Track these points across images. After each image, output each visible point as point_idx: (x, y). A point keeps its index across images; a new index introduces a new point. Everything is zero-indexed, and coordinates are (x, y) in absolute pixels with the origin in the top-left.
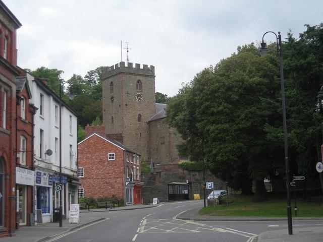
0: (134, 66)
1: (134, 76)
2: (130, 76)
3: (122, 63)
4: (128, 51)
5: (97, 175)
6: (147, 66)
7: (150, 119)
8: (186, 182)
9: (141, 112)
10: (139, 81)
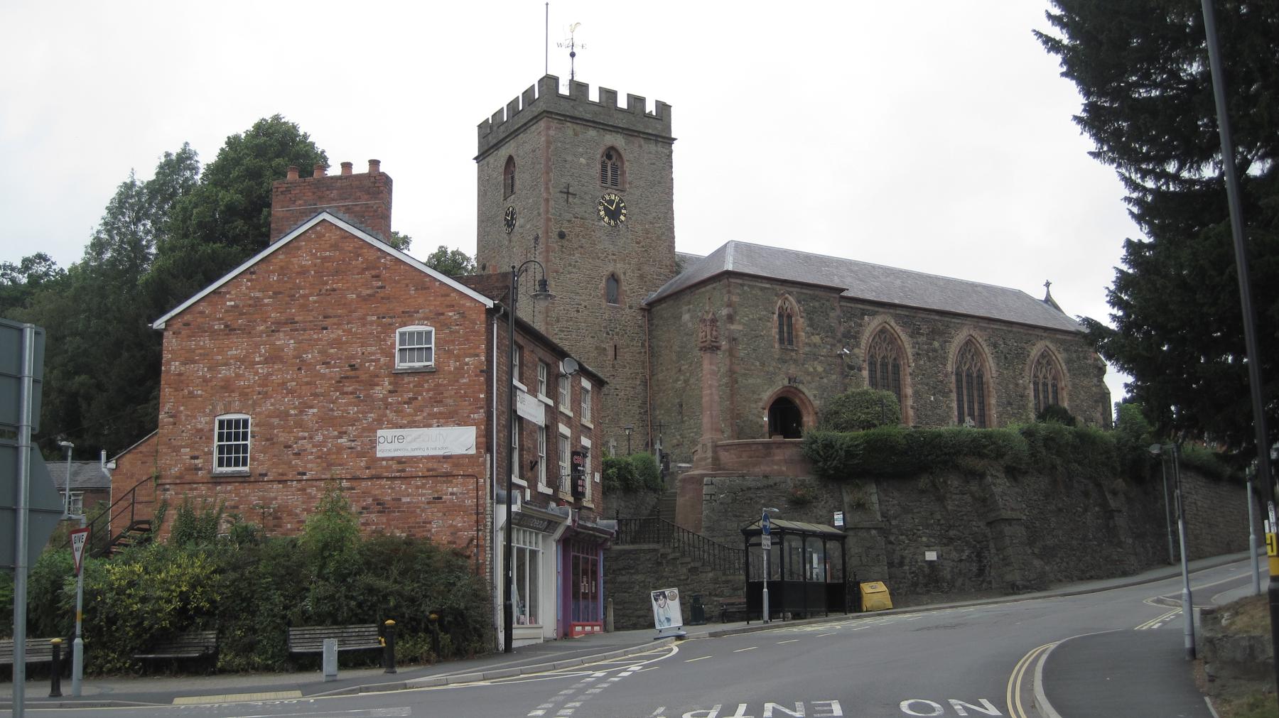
0: (594, 96)
1: (592, 133)
2: (578, 128)
3: (549, 82)
4: (573, 55)
5: (327, 461)
6: (641, 100)
7: (654, 295)
8: (830, 522)
9: (619, 268)
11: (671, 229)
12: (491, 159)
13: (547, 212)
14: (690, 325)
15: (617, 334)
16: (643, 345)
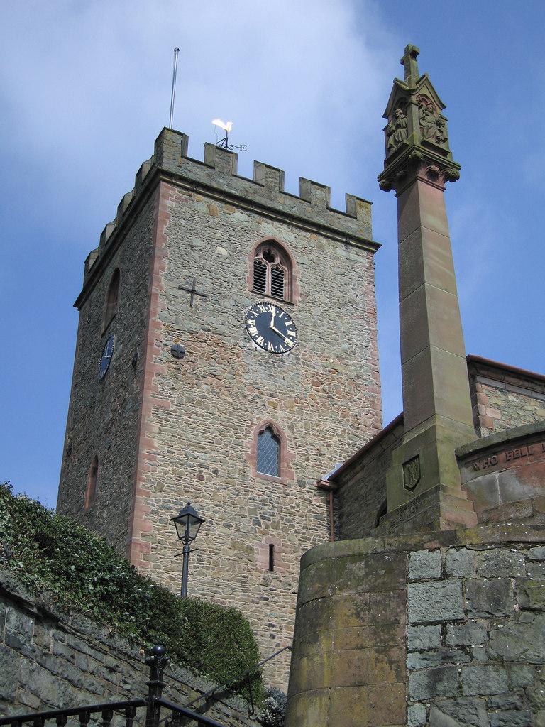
1: (239, 216)
2: (217, 205)
9: (281, 419)
10: (271, 249)
12: (95, 294)
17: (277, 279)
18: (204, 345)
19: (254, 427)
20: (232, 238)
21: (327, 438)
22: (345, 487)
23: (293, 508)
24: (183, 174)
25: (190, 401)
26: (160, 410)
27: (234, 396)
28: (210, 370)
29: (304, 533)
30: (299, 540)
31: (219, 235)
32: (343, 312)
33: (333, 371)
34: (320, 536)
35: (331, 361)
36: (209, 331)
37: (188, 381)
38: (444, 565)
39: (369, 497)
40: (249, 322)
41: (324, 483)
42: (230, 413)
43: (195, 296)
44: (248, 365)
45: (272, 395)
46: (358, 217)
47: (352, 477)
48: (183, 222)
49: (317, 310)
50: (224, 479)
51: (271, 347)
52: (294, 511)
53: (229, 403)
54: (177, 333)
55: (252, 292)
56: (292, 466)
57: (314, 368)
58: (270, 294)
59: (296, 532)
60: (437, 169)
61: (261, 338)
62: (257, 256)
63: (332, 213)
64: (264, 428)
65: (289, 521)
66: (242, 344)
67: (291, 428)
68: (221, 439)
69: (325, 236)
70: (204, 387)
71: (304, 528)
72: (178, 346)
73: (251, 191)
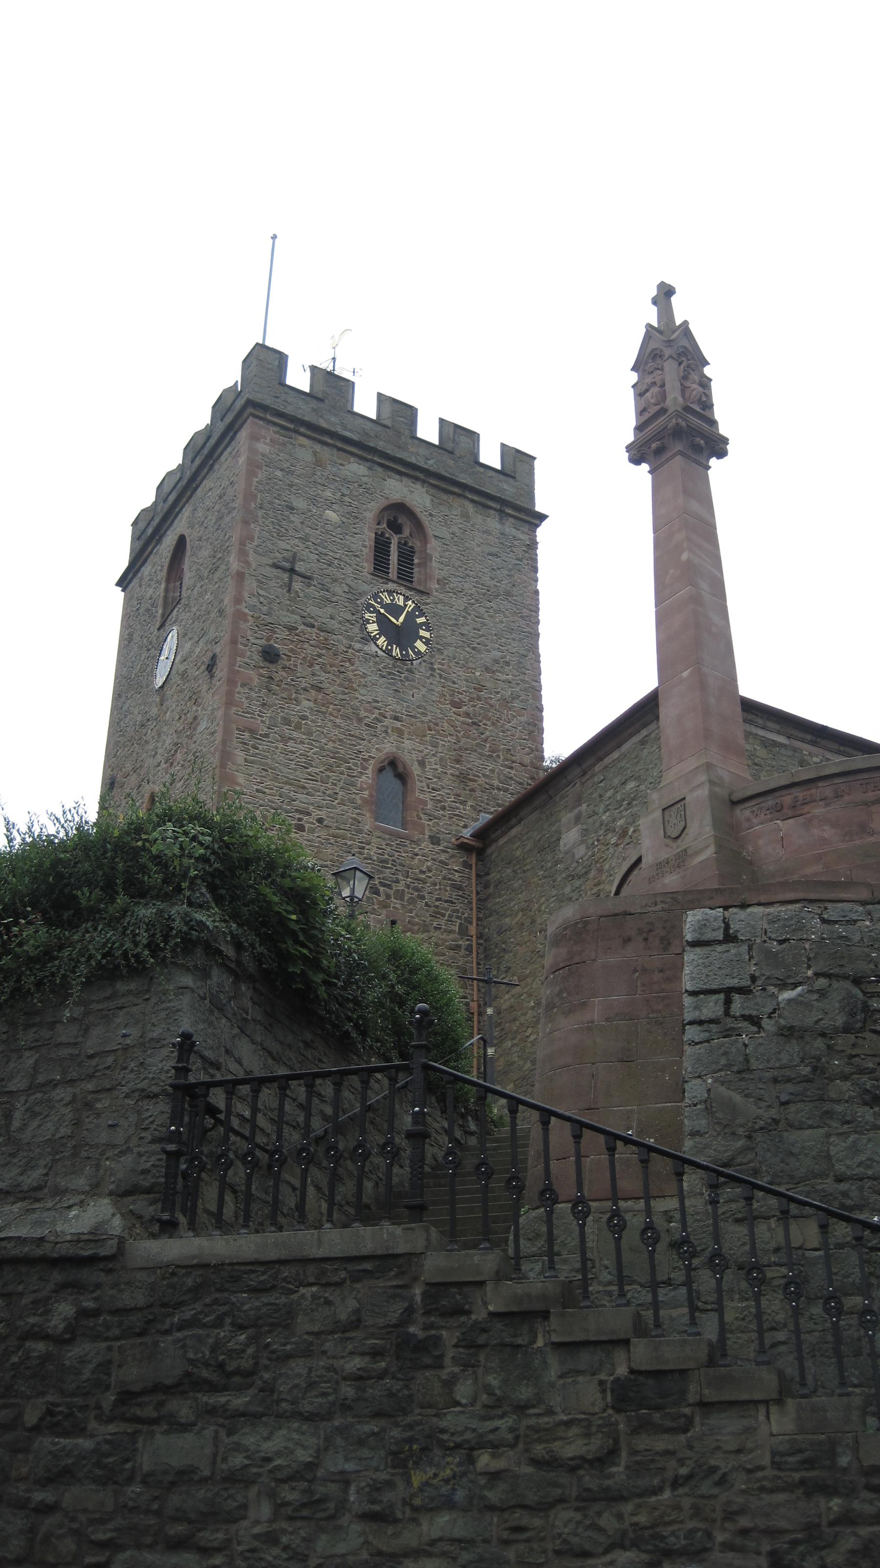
1: (356, 469)
2: (326, 453)
9: (409, 751)
10: (397, 515)
11: (535, 691)
12: (146, 570)
13: (238, 600)
14: (581, 851)
15: (400, 895)
16: (463, 931)
17: (406, 557)
18: (306, 646)
19: (372, 762)
20: (346, 499)
21: (471, 780)
22: (493, 847)
23: (422, 872)
24: (281, 408)
25: (287, 722)
26: (247, 734)
27: (346, 717)
28: (314, 681)
29: (437, 907)
30: (431, 916)
31: (328, 494)
32: (495, 607)
33: (480, 688)
34: (457, 911)
35: (478, 674)
36: (313, 626)
37: (284, 695)
38: (727, 927)
39: (528, 861)
40: (367, 616)
41: (466, 841)
42: (340, 740)
43: (295, 577)
44: (364, 676)
45: (396, 718)
46: (517, 477)
47: (504, 833)
48: (279, 473)
49: (460, 603)
50: (331, 831)
51: (396, 652)
52: (423, 876)
53: (339, 727)
54: (270, 627)
55: (372, 574)
56: (422, 816)
57: (454, 683)
58: (395, 578)
59: (427, 905)
60: (702, 442)
61: (383, 639)
62: (378, 524)
63: (482, 470)
64: (386, 763)
65: (418, 890)
66: (357, 646)
67: (422, 763)
68: (328, 777)
69: (472, 501)
70: (306, 703)
71: (437, 899)
72: (271, 646)
73: (372, 434)
